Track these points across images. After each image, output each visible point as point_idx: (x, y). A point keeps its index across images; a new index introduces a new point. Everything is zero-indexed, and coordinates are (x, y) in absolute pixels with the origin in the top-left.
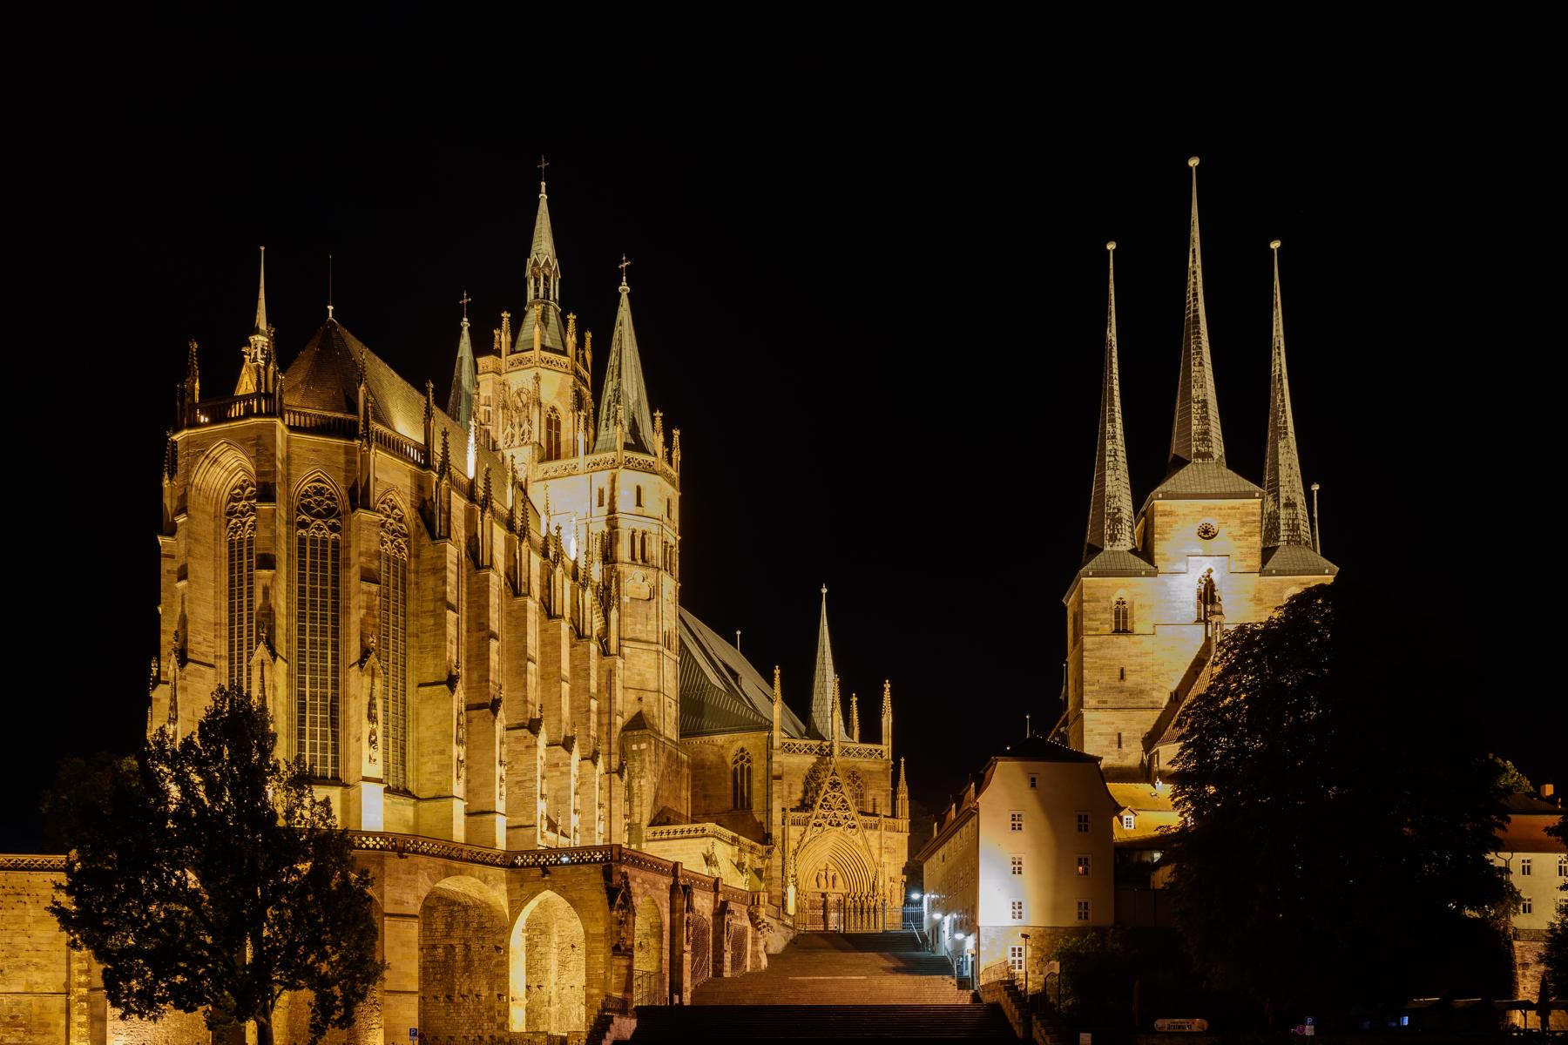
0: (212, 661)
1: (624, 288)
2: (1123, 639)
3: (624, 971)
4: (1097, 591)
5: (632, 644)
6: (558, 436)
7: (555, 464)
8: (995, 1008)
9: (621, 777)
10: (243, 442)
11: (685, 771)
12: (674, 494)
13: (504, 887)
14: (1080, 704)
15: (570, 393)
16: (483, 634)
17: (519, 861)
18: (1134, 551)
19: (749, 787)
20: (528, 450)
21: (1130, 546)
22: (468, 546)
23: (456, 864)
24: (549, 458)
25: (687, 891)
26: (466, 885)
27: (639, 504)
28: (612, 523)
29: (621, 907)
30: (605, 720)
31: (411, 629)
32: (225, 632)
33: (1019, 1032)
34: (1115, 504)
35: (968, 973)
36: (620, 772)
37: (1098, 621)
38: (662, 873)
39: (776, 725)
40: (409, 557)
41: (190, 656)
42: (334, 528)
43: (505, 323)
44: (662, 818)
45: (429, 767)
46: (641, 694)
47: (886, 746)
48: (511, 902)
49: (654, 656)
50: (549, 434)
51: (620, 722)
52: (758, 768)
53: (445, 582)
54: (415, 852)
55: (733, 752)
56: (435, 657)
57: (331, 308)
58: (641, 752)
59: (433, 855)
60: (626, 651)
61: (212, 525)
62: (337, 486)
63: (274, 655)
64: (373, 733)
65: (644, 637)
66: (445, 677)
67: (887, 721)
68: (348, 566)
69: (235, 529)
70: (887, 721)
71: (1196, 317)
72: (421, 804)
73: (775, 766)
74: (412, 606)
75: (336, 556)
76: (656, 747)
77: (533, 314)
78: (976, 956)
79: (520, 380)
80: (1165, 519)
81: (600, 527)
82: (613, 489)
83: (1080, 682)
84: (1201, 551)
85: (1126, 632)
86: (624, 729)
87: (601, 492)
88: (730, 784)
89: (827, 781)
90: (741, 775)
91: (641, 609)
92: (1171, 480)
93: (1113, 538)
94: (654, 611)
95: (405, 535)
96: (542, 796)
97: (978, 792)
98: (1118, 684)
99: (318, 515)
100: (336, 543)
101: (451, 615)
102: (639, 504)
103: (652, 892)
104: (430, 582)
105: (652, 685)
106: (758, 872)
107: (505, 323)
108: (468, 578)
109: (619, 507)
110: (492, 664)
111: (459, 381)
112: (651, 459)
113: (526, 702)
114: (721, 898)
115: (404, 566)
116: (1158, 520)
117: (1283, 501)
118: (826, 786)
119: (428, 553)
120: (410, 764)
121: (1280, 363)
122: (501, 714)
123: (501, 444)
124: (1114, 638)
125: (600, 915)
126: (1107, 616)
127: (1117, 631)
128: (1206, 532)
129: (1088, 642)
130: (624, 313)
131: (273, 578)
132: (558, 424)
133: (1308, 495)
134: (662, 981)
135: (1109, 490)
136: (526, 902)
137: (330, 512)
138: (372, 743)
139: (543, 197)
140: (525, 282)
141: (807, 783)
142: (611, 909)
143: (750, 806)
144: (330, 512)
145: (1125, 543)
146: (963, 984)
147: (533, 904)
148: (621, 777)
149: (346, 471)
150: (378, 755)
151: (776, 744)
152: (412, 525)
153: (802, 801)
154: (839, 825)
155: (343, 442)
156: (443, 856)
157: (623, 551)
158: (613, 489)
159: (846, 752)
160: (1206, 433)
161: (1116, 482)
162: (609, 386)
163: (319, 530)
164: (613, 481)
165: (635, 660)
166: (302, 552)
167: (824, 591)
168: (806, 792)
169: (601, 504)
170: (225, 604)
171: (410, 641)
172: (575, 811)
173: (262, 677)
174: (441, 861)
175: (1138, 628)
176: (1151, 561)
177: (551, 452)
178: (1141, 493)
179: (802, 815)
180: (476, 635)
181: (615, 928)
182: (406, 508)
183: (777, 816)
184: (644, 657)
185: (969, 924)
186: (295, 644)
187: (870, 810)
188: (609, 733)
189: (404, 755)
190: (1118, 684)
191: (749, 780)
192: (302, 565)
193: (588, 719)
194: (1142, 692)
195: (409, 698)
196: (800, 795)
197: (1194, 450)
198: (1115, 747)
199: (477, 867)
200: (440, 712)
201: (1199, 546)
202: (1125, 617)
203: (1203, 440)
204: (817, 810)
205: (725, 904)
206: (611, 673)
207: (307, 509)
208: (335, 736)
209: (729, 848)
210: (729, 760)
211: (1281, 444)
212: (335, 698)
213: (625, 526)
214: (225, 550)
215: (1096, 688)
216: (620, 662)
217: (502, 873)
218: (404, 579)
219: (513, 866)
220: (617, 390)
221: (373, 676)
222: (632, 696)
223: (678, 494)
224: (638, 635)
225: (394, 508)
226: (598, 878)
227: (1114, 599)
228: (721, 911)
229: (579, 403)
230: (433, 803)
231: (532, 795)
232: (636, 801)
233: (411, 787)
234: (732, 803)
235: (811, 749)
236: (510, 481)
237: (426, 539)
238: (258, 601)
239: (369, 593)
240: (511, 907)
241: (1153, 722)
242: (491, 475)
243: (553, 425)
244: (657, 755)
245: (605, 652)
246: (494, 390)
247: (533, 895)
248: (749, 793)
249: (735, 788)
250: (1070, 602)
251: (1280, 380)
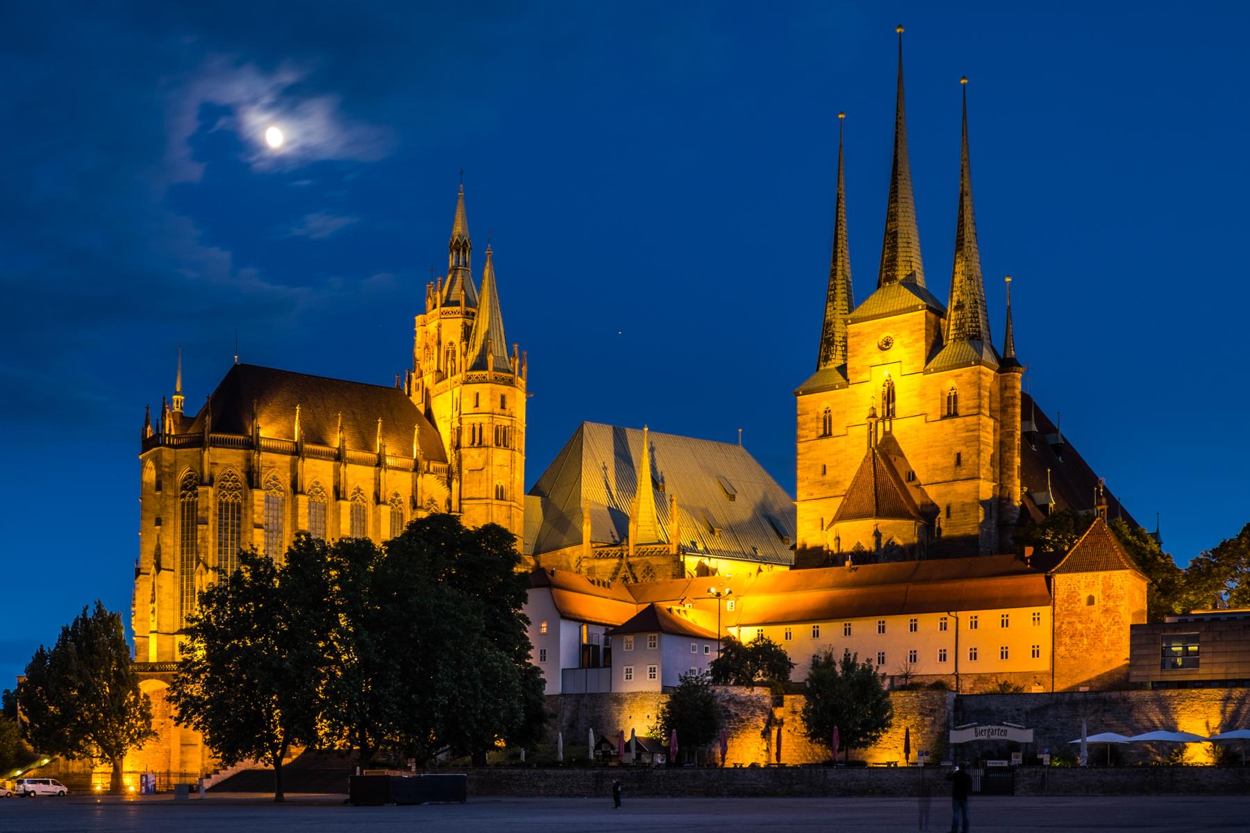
2: (825, 441)
37: (808, 427)
98: (821, 478)
157: (466, 439)
176: (845, 376)
190: (821, 478)
194: (837, 483)
201: (877, 358)
215: (806, 483)
224: (474, 495)
227: (821, 411)
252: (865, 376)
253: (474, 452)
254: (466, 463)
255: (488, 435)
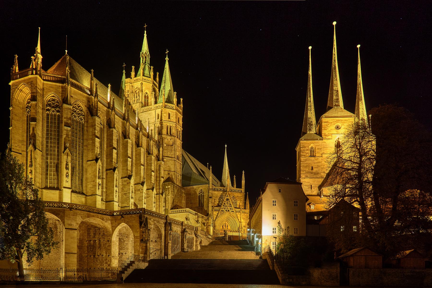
0: (21, 152)
1: (167, 59)
3: (144, 248)
4: (305, 145)
5: (167, 158)
6: (148, 101)
7: (146, 108)
8: (265, 260)
9: (162, 195)
10: (27, 83)
11: (184, 195)
12: (181, 116)
13: (110, 222)
14: (300, 177)
15: (151, 88)
16: (111, 148)
17: (115, 214)
18: (316, 133)
19: (203, 200)
20: (138, 104)
21: (315, 132)
22: (107, 122)
23: (92, 214)
24: (145, 106)
25: (170, 224)
26: (96, 221)
27: (169, 118)
28: (161, 123)
29: (143, 227)
30: (158, 179)
31: (85, 144)
32: (25, 144)
33: (271, 268)
34: (311, 120)
35: (259, 251)
36: (162, 194)
38: (162, 218)
39: (211, 183)
40: (85, 122)
41: (12, 150)
42: (58, 111)
43: (133, 69)
44: (174, 207)
45: (90, 186)
46: (169, 172)
47: (243, 189)
48: (112, 227)
49: (173, 161)
50: (145, 100)
51: (162, 180)
52: (206, 195)
53: (95, 129)
54: (76, 209)
55: (199, 190)
56: (92, 152)
57: (66, 51)
58: (168, 188)
59: (83, 210)
60: (165, 160)
61: (22, 111)
62: (58, 98)
63: (35, 148)
64: (67, 173)
65: (170, 156)
66: (95, 158)
67: (243, 182)
68: (62, 123)
69: (28, 112)
70: (243, 182)
71: (335, 67)
72: (88, 197)
73: (210, 194)
74: (85, 137)
75: (59, 119)
76: (174, 187)
77: (142, 66)
78: (261, 245)
79: (137, 85)
80: (326, 124)
81: (158, 125)
82: (162, 114)
83: (300, 171)
84: (336, 133)
85: (314, 156)
86: (164, 182)
87: (158, 115)
88: (198, 200)
89: (226, 198)
90: (201, 197)
91: (170, 148)
92: (327, 113)
93: (310, 130)
94: (173, 149)
95: (83, 115)
96: (132, 198)
97: (262, 193)
98: (311, 171)
99: (53, 107)
100: (59, 116)
101: (129, 160)
102: (169, 118)
103: (157, 224)
104: (91, 129)
105: (173, 170)
106: (204, 224)
107: (133, 69)
108: (107, 131)
109: (163, 119)
110: (114, 157)
111: (122, 88)
112: (172, 105)
113: (127, 170)
114: (184, 228)
115: (83, 125)
116: (323, 124)
117: (360, 119)
118: (225, 200)
119: (90, 121)
120: (84, 185)
121: (360, 79)
122: (116, 171)
123: (131, 103)
124: (310, 158)
125: (138, 230)
126: (308, 152)
127: (311, 156)
128: (338, 127)
129: (302, 159)
130: (167, 66)
131: (36, 125)
132: (148, 97)
133: (368, 118)
134: (161, 252)
135: (309, 116)
136: (117, 227)
137: (57, 106)
138: (67, 176)
139: (145, 35)
140: (140, 59)
141: (219, 199)
142: (140, 228)
143: (203, 206)
144: (57, 106)
145: (313, 131)
146: (258, 254)
147: (119, 227)
148: (162, 195)
149: (62, 93)
150: (69, 179)
151: (211, 188)
152: (86, 112)
153: (218, 204)
154: (229, 211)
155: (61, 85)
156: (87, 211)
157: (164, 131)
158: (162, 114)
159: (231, 191)
160: (338, 99)
161: (311, 114)
162: (162, 86)
163: (53, 112)
164: (162, 111)
165: (168, 163)
166: (48, 118)
167: (226, 146)
168: (219, 202)
169: (158, 118)
170: (25, 135)
171: (85, 148)
172: (145, 203)
173: (31, 155)
174: (86, 212)
175: (317, 155)
176: (321, 136)
177: (146, 104)
178: (318, 116)
179: (218, 208)
180: (109, 148)
181: (141, 234)
182: (84, 108)
183: (210, 208)
184: (170, 162)
185: (260, 237)
186: (45, 146)
187: (238, 207)
188: (159, 183)
189: (82, 182)
190: (311, 171)
191: (203, 198)
192: (48, 122)
193: (151, 178)
194: (318, 173)
195: (84, 165)
196: (217, 203)
197: (334, 104)
198: (310, 189)
199: (100, 215)
200: (93, 169)
202: (313, 152)
203: (337, 101)
204: (222, 207)
205: (185, 229)
206: (160, 166)
207: (49, 105)
208: (58, 175)
209: (194, 216)
210: (198, 193)
211: (360, 102)
212: (58, 164)
213: (164, 124)
214: (26, 119)
216: (163, 163)
217: (109, 217)
218: (83, 129)
219: (113, 215)
220: (164, 87)
221: (68, 155)
222: (166, 173)
223: (182, 117)
224: (169, 155)
225: (79, 107)
226: (137, 219)
228: (183, 231)
229: (154, 90)
230: (91, 197)
231: (129, 197)
232: (167, 203)
233: (84, 192)
234: (199, 206)
235: (221, 190)
236: (124, 105)
237: (90, 117)
238: (31, 132)
239: (67, 130)
240: (112, 228)
241: (321, 182)
242: (115, 101)
243: (146, 97)
244: (174, 189)
245: (158, 159)
246: (130, 88)
247: (119, 224)
248: (203, 202)
249: (199, 201)
250: (297, 149)
251: (360, 84)
252: (330, 137)
253: (169, 138)
254: (166, 141)
255: (174, 131)
